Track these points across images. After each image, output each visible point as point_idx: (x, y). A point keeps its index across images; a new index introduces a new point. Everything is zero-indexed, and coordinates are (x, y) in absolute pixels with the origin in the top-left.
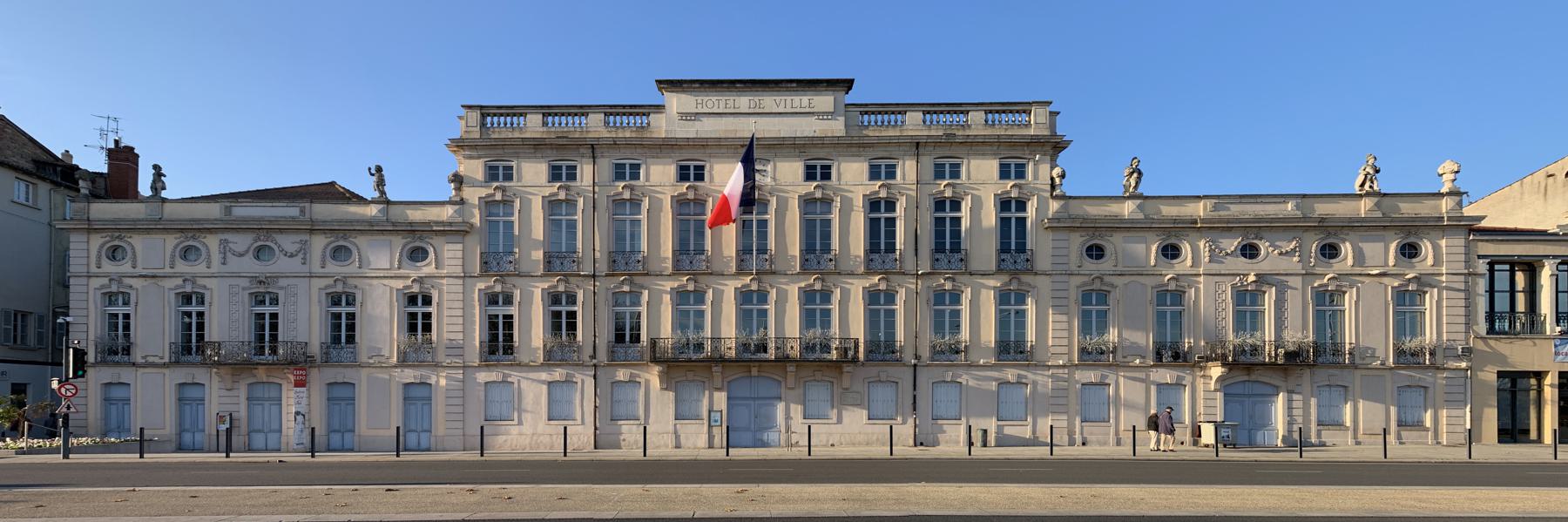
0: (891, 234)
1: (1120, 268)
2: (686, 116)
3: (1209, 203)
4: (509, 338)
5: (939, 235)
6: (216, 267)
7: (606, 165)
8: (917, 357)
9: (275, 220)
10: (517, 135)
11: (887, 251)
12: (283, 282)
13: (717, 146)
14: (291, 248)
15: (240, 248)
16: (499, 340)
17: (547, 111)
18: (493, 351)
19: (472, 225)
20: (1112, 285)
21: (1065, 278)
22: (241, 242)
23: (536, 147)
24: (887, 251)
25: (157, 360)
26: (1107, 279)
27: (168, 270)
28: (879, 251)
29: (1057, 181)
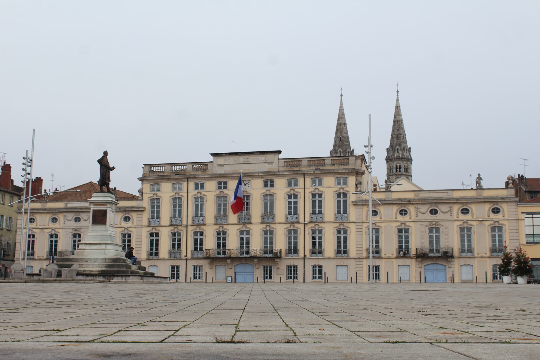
0: (296, 208)
1: (383, 219)
2: (221, 166)
3: (413, 193)
4: (157, 249)
5: (314, 207)
6: (62, 225)
7: (192, 185)
8: (305, 256)
9: (81, 208)
10: (162, 174)
11: (294, 214)
12: (82, 230)
13: (231, 176)
14: (86, 218)
15: (69, 218)
16: (154, 251)
17: (172, 165)
18: (151, 254)
19: (145, 208)
20: (379, 226)
21: (361, 224)
22: (71, 216)
23: (169, 179)
24: (294, 214)
25: (42, 258)
26: (377, 224)
27: (47, 226)
28: (291, 214)
29: (358, 186)
